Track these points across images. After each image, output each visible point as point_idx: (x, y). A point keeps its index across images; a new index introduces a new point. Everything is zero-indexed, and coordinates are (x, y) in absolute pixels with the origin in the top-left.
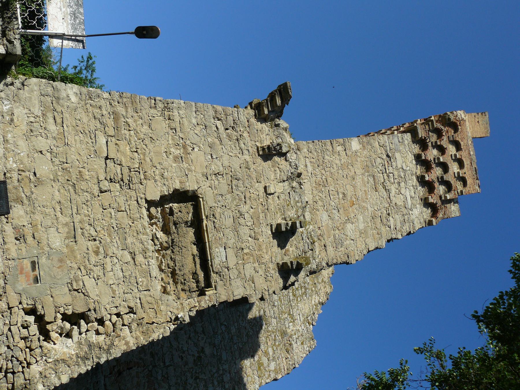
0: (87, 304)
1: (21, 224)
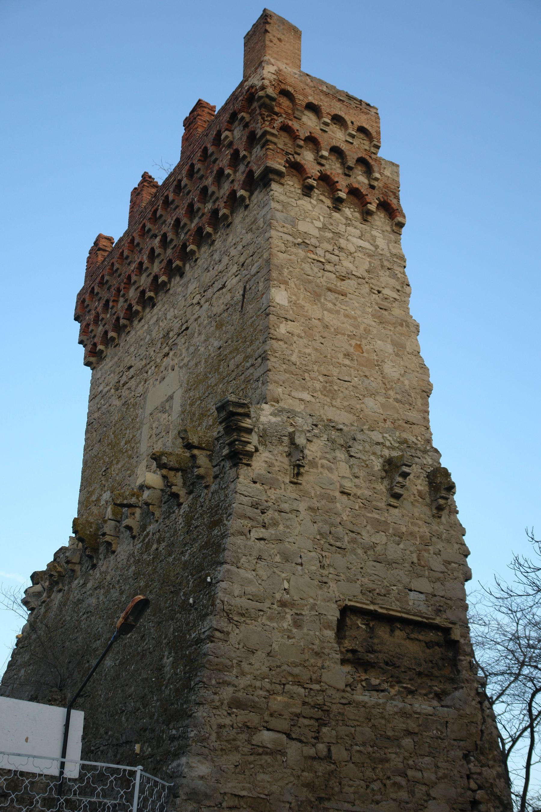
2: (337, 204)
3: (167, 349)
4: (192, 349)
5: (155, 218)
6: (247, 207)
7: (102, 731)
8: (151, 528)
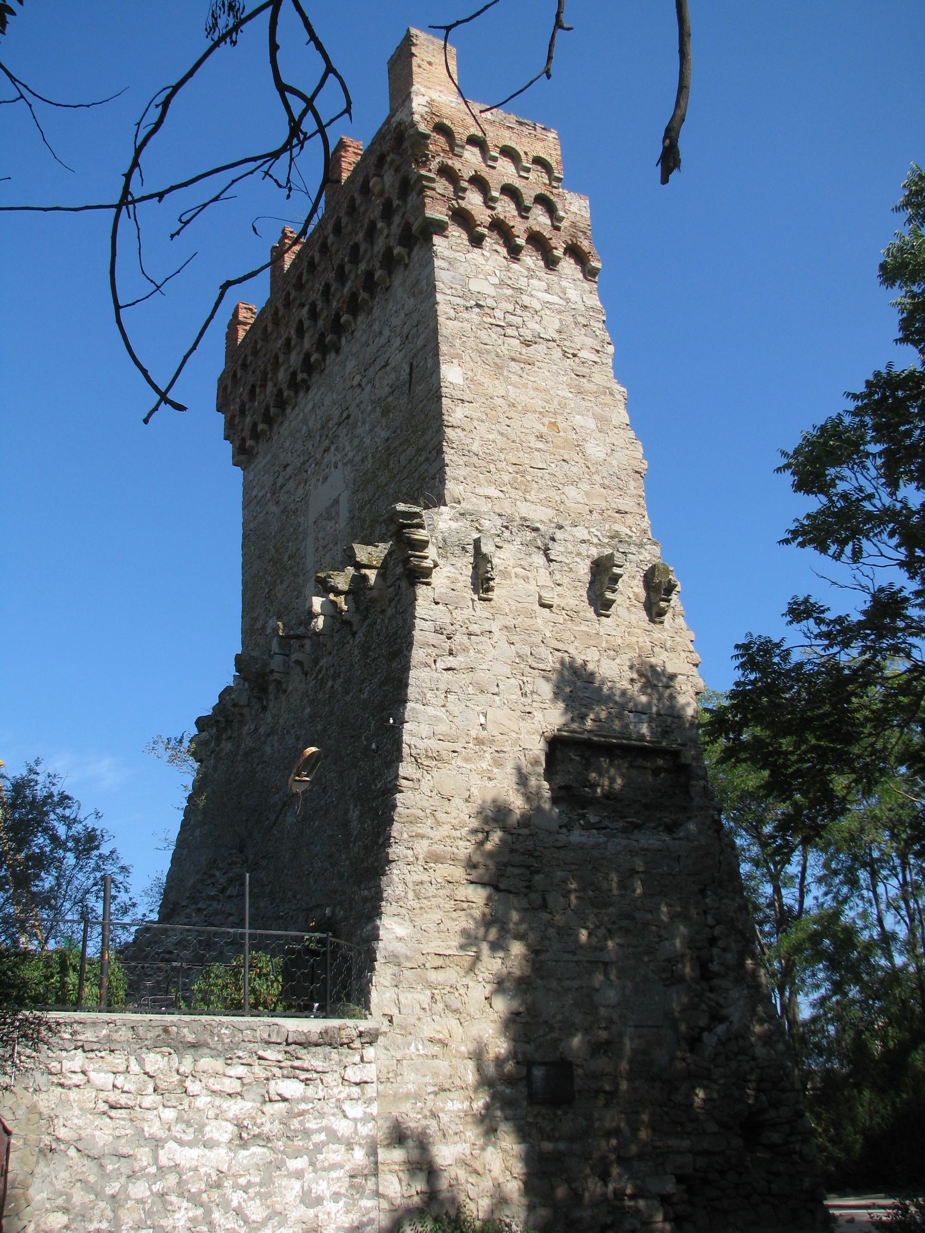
3: (326, 443)
4: (356, 442)
5: (300, 286)
6: (406, 266)
7: (290, 894)
8: (323, 662)
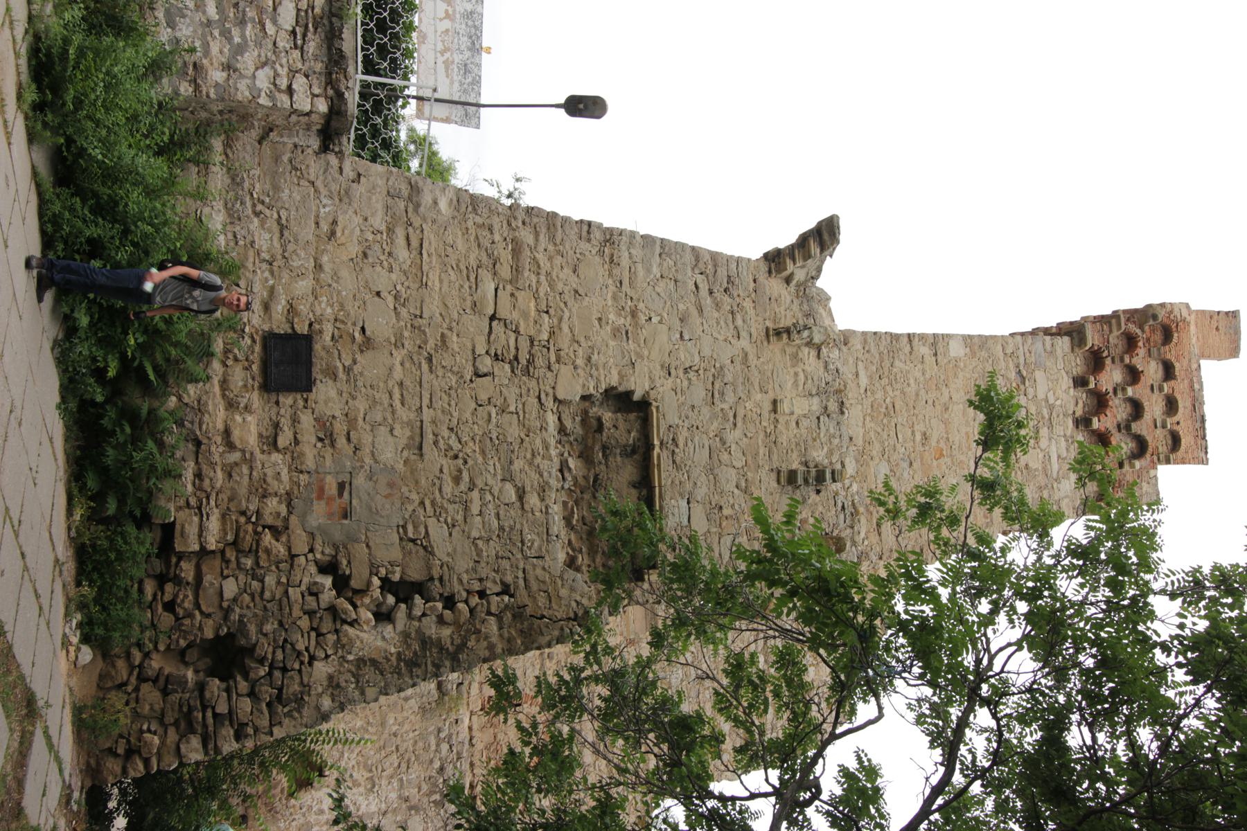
0: (429, 568)
1: (328, 413)
2: (1083, 422)
